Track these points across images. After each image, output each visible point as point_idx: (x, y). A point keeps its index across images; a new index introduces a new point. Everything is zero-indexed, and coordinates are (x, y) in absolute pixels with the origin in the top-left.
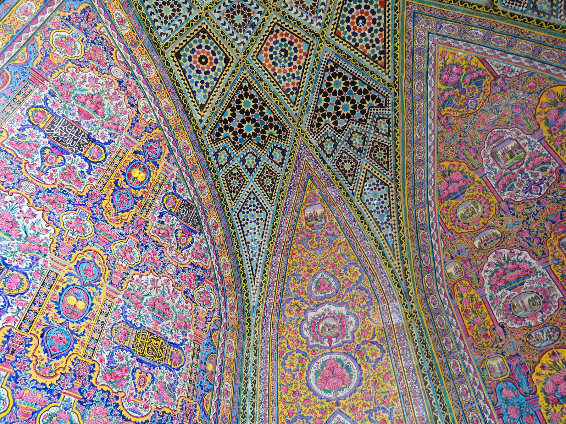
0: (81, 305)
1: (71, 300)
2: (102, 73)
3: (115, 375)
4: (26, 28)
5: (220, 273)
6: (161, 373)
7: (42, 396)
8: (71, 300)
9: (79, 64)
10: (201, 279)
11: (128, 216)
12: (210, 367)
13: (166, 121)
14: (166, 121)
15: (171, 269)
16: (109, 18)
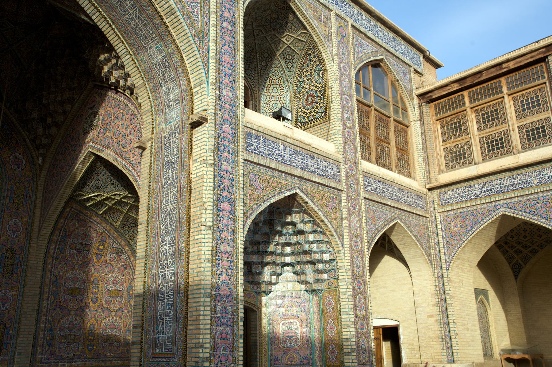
0: (97, 290)
1: (94, 290)
2: (84, 227)
3: (108, 303)
4: (63, 226)
5: (132, 263)
6: (119, 299)
7: (95, 312)
8: (94, 290)
9: (78, 228)
10: (126, 268)
11: (101, 260)
12: (131, 293)
13: (106, 230)
14: (106, 230)
15: (116, 270)
16: (83, 213)
